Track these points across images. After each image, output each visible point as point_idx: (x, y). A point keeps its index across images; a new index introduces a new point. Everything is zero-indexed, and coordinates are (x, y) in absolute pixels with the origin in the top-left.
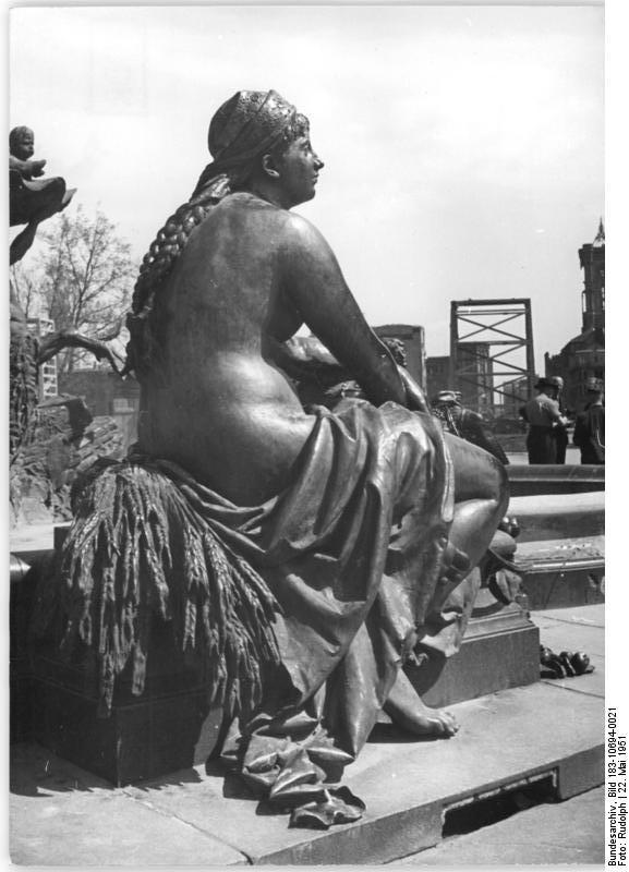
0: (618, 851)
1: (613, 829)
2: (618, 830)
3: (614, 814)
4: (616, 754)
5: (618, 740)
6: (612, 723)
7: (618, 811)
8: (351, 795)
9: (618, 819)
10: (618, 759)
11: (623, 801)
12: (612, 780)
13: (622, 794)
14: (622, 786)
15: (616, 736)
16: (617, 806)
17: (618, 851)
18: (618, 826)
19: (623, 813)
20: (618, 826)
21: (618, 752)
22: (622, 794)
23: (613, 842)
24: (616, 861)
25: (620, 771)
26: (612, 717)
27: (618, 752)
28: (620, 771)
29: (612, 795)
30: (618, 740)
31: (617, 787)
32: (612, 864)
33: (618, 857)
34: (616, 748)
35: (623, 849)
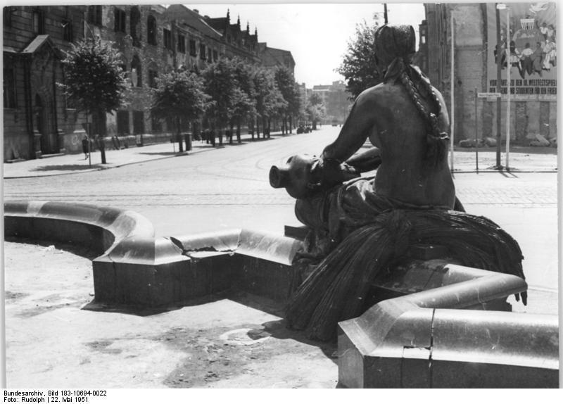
0: (14, 397)
1: (27, 394)
2: (27, 397)
3: (38, 394)
4: (76, 396)
5: (85, 397)
6: (96, 393)
7: (40, 397)
8: (231, 298)
9: (34, 397)
10: (73, 397)
11: (46, 400)
12: (60, 394)
13: (51, 400)
14: (55, 399)
15: (88, 395)
16: (43, 396)
17: (14, 397)
18: (30, 397)
19: (38, 400)
20: (30, 397)
21: (78, 397)
22: (51, 400)
23: (20, 394)
24: (7, 396)
25: (65, 398)
26: (100, 393)
27: (78, 397)
28: (65, 398)
29: (50, 393)
30: (85, 397)
31: (55, 396)
32: (5, 393)
33: (10, 397)
34: (80, 396)
35: (15, 400)
